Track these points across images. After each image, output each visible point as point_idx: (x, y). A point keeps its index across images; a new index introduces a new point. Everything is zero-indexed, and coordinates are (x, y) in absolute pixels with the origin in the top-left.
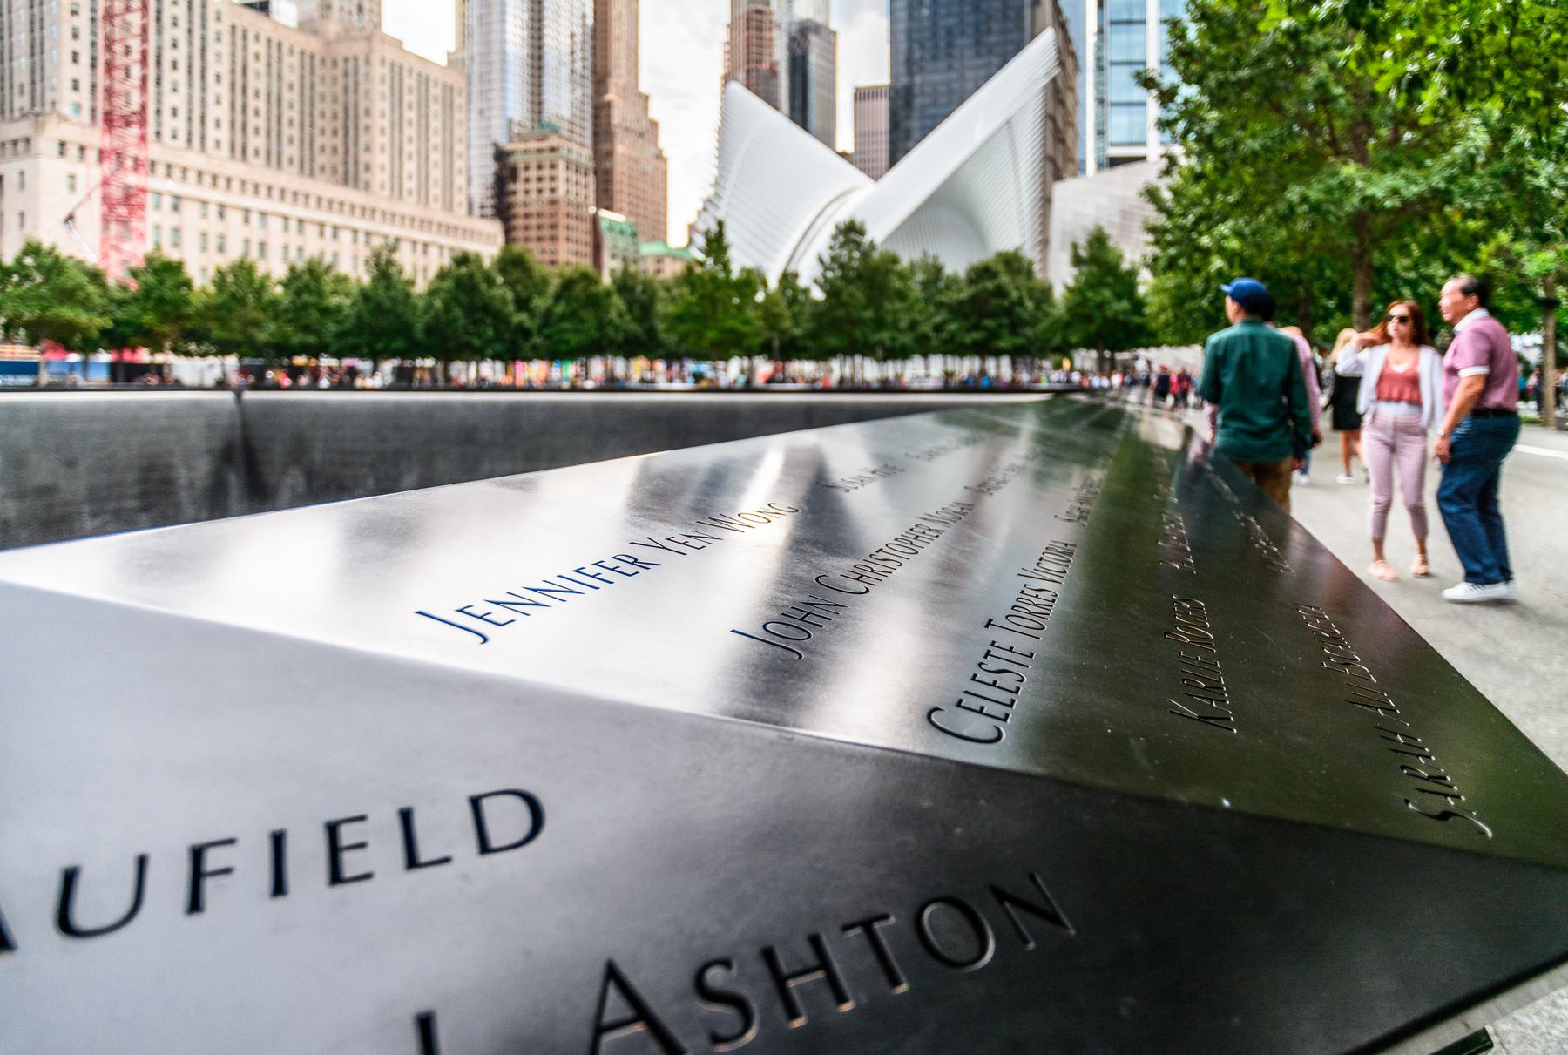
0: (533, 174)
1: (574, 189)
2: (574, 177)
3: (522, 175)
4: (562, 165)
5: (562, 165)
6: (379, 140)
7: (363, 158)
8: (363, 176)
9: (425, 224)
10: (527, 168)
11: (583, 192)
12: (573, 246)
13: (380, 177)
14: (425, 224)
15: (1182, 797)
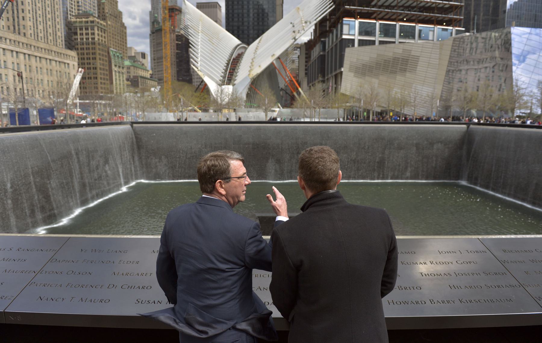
0: (84, 32)
1: (101, 38)
2: (100, 33)
3: (79, 32)
4: (96, 29)
5: (96, 29)
6: (28, 16)
7: (22, 22)
8: (22, 31)
9: (50, 51)
10: (81, 29)
11: (104, 40)
12: (101, 62)
13: (29, 32)
14: (50, 51)
15: (341, 173)
